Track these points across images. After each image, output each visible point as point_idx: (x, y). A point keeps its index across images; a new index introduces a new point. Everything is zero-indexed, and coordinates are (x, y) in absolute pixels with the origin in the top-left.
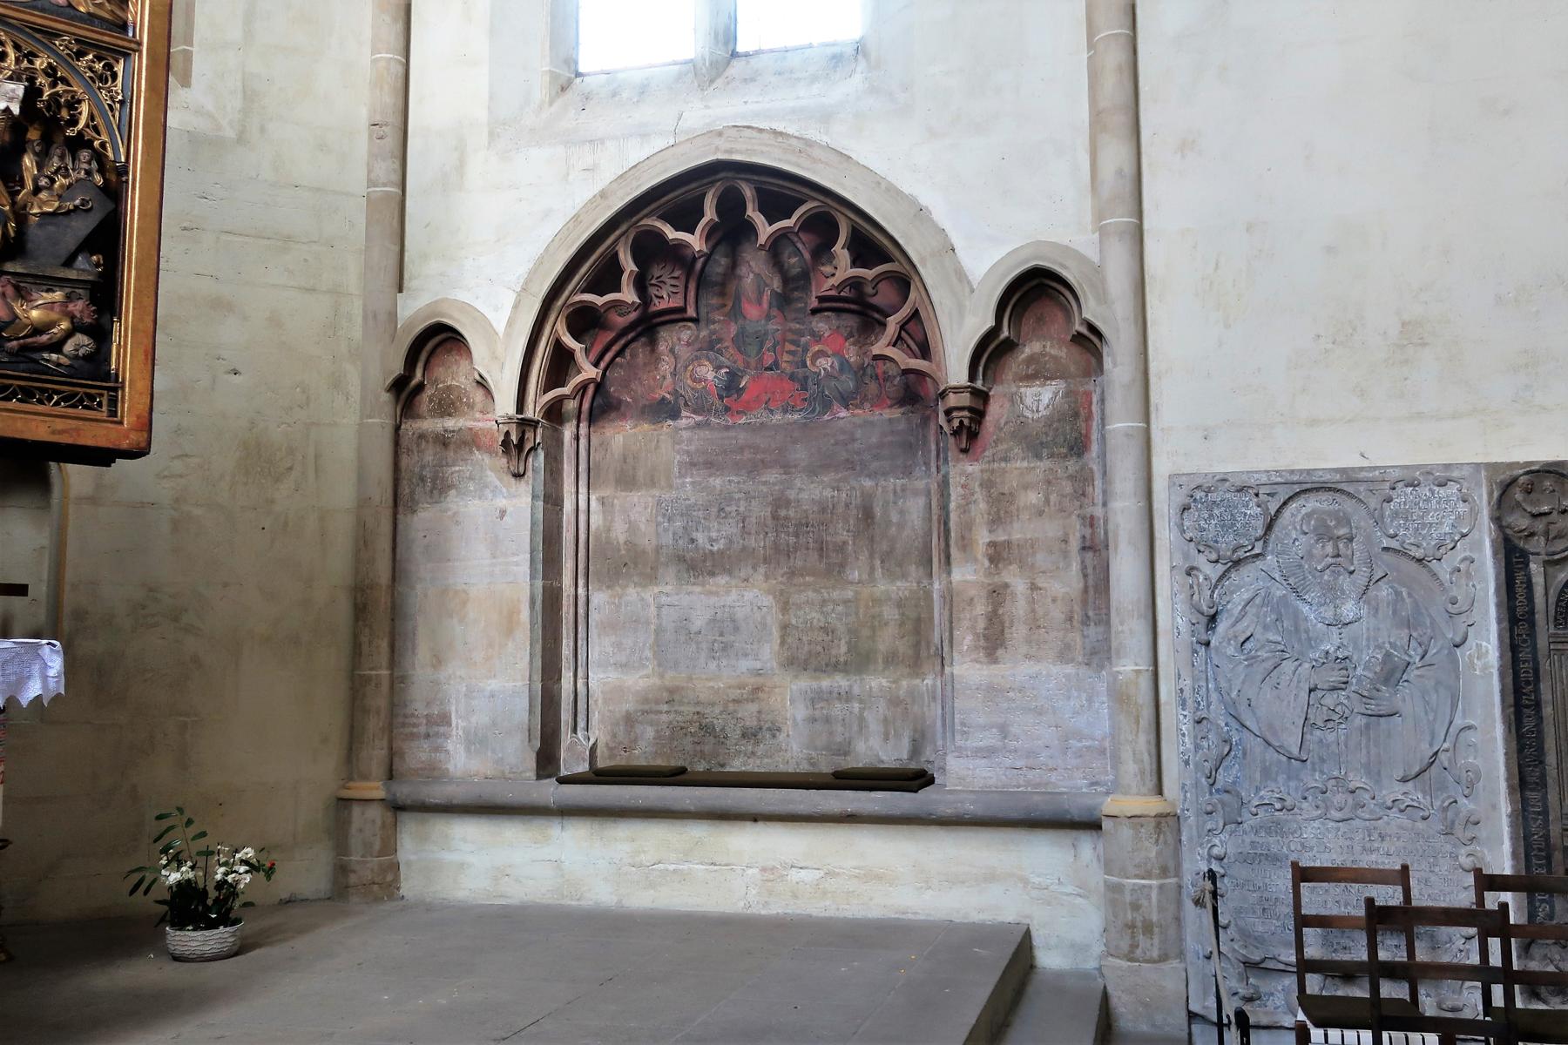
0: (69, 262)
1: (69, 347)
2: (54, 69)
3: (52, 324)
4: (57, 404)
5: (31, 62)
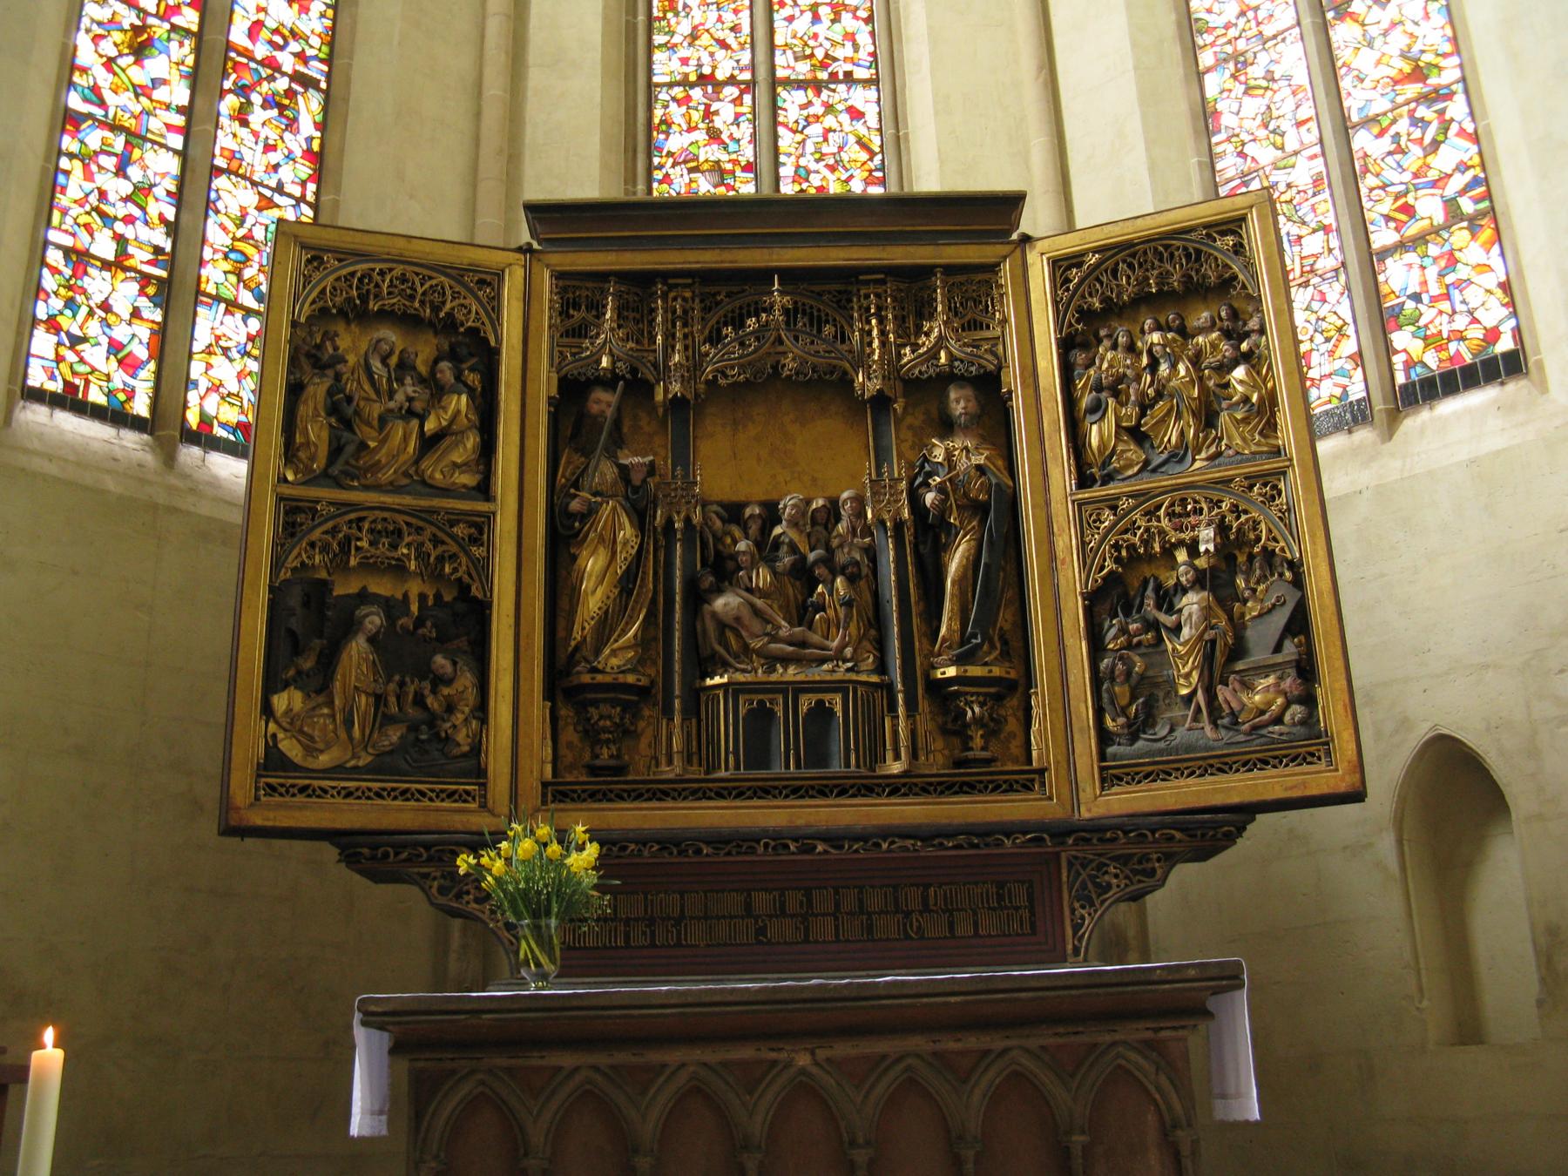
0: (1278, 648)
1: (1287, 718)
2: (1236, 506)
3: (1270, 704)
4: (1287, 765)
5: (1220, 507)
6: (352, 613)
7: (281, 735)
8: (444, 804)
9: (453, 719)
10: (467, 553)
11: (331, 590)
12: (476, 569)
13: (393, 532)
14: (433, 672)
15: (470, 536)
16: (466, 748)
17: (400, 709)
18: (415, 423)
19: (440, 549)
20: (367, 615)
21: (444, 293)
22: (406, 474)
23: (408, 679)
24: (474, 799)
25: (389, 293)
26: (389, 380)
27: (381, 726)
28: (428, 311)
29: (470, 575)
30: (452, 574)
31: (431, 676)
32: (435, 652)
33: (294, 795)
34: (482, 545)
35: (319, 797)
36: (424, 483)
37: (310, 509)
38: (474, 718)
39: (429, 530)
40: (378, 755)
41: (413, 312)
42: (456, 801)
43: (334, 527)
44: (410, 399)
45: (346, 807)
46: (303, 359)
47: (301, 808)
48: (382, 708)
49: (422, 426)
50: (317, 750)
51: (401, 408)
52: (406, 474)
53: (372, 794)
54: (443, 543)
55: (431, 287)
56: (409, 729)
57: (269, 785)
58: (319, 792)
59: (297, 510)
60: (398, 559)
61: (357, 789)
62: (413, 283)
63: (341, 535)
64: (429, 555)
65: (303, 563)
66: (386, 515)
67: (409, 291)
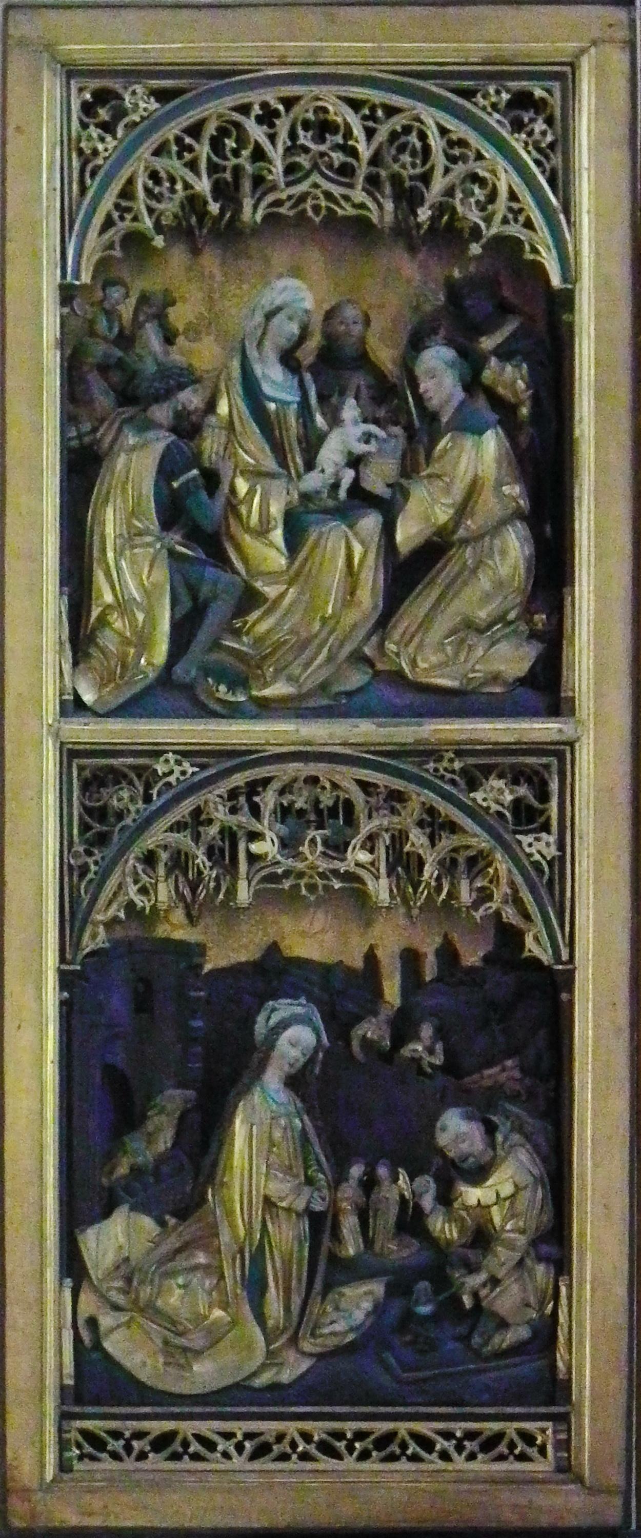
6: (248, 1022)
7: (106, 1321)
8: (473, 1466)
9: (490, 1262)
10: (507, 848)
11: (200, 966)
12: (533, 890)
13: (333, 812)
14: (441, 1152)
15: (517, 804)
16: (524, 1333)
17: (369, 1243)
18: (371, 522)
19: (447, 842)
20: (284, 1025)
21: (426, 150)
22: (359, 658)
23: (382, 1171)
24: (542, 1451)
25: (290, 169)
26: (304, 404)
27: (328, 1288)
28: (389, 206)
29: (517, 901)
30: (476, 905)
31: (437, 1161)
32: (444, 1103)
33: (142, 1456)
34: (546, 828)
35: (196, 1457)
36: (398, 678)
37: (139, 770)
38: (540, 1259)
39: (420, 796)
40: (320, 1357)
41: (350, 211)
42: (501, 1458)
43: (197, 812)
44: (355, 462)
45: (252, 1479)
46: (94, 378)
47: (159, 1485)
48: (326, 1242)
49: (388, 529)
50: (185, 1350)
51: (335, 486)
52: (359, 658)
53: (312, 1449)
54: (453, 827)
55: (394, 136)
56: (391, 1291)
58: (195, 1447)
59: (117, 777)
60: (349, 877)
61: (280, 1438)
62: (348, 134)
63: (213, 830)
64: (421, 863)
65: (130, 906)
66: (312, 769)
67: (338, 158)
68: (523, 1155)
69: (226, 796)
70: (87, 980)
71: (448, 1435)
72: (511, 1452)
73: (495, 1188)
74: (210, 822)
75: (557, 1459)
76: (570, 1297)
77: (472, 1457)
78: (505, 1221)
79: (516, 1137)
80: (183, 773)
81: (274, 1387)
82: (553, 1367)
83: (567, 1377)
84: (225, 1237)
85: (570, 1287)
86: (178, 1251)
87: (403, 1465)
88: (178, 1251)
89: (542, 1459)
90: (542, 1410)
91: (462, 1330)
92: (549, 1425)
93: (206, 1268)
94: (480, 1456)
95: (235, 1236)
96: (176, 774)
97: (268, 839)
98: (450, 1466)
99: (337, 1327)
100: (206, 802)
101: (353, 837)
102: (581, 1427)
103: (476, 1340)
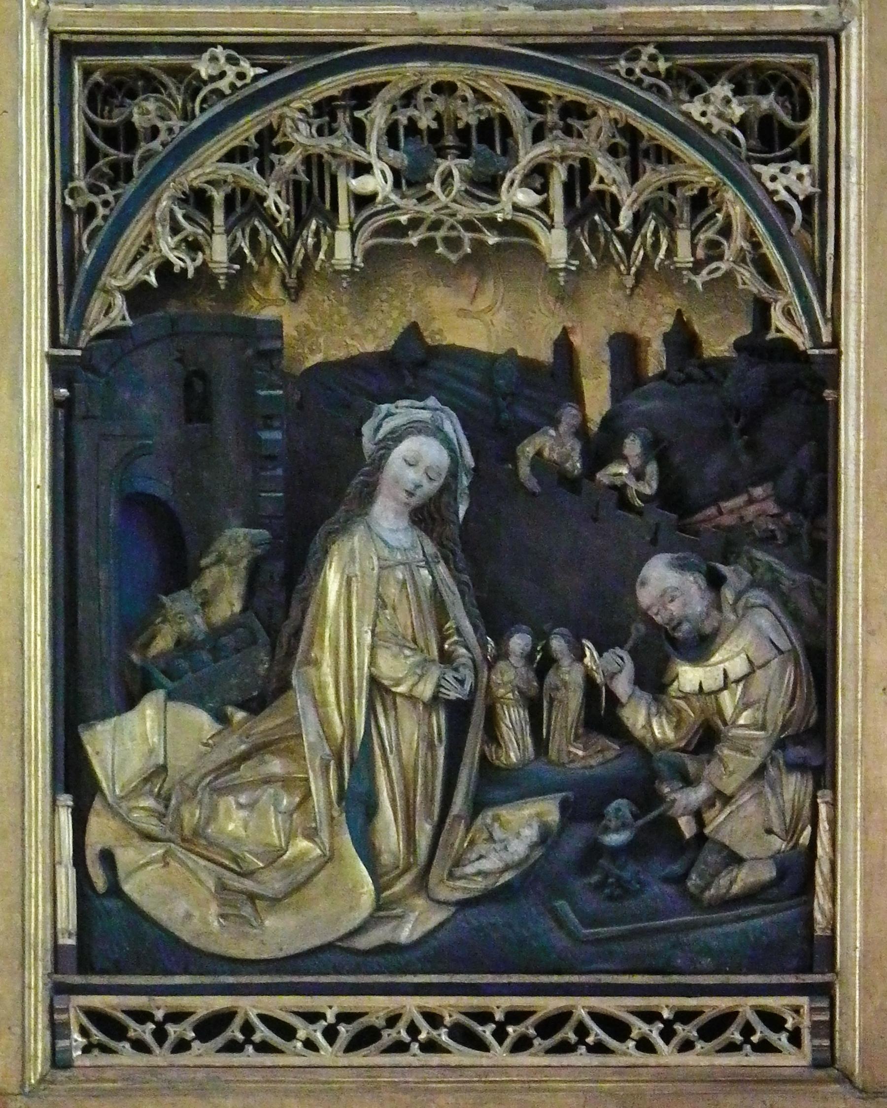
8: (689, 1059)
16: (767, 873)
42: (732, 1048)
43: (267, 135)
57: (97, 1017)
63: (291, 160)
68: (764, 620)
69: (310, 109)
70: (94, 370)
71: (649, 1016)
72: (747, 1041)
73: (722, 666)
74: (287, 147)
75: (815, 1049)
76: (833, 822)
77: (686, 1046)
78: (738, 713)
79: (757, 596)
80: (241, 76)
81: (389, 948)
82: (810, 919)
83: (828, 933)
84: (310, 733)
85: (833, 804)
86: (245, 757)
87: (581, 1058)
88: (245, 757)
89: (793, 1049)
90: (791, 979)
91: (676, 868)
92: (803, 1001)
93: (286, 782)
94: (699, 1045)
95: (327, 736)
96: (231, 77)
97: (377, 171)
98: (651, 1059)
99: (486, 865)
100: (282, 117)
101: (508, 169)
102: (848, 999)
103: (694, 881)
